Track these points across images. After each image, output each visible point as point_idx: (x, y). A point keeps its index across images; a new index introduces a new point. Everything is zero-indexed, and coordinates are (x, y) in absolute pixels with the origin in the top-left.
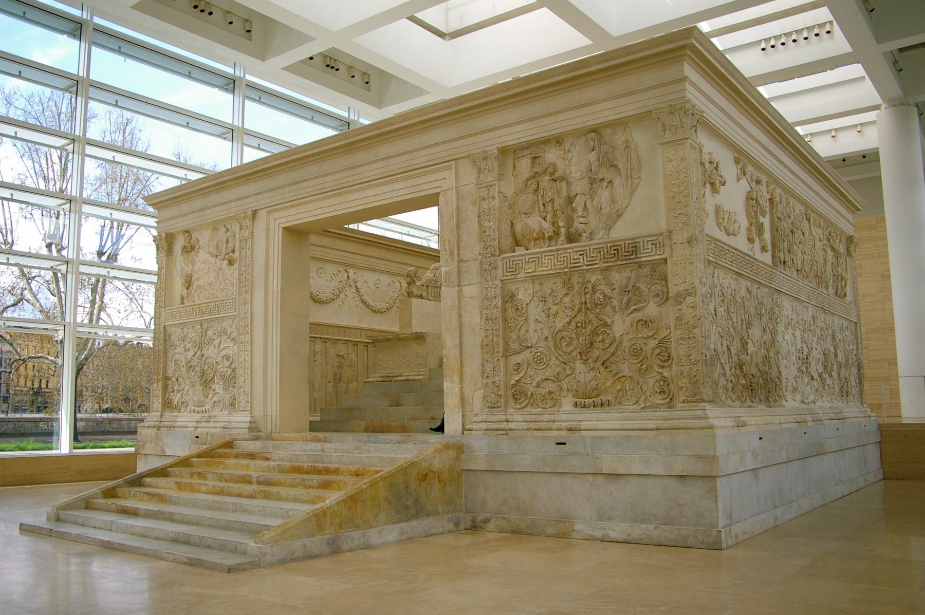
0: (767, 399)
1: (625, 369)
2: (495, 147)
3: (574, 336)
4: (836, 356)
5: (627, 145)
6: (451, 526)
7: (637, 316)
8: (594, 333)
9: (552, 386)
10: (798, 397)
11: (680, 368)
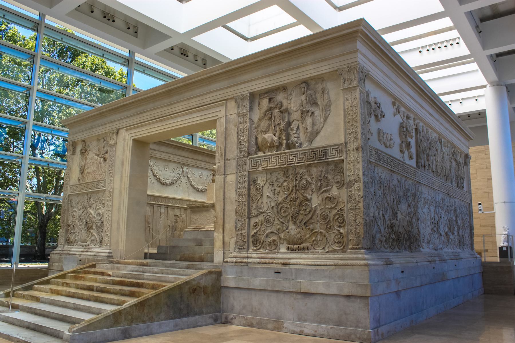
0: (410, 247)
4: (457, 222)
5: (323, 90)
6: (211, 321)
7: (326, 195)
8: (300, 205)
9: (275, 237)
10: (431, 246)
11: (349, 227)
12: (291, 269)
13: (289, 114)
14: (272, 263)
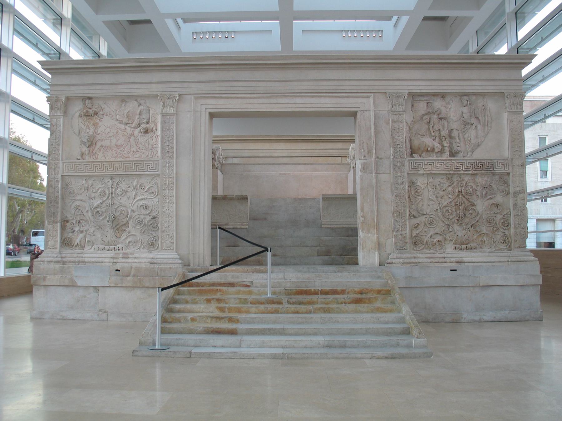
1: (484, 229)
2: (407, 91)
5: (485, 108)
8: (466, 209)
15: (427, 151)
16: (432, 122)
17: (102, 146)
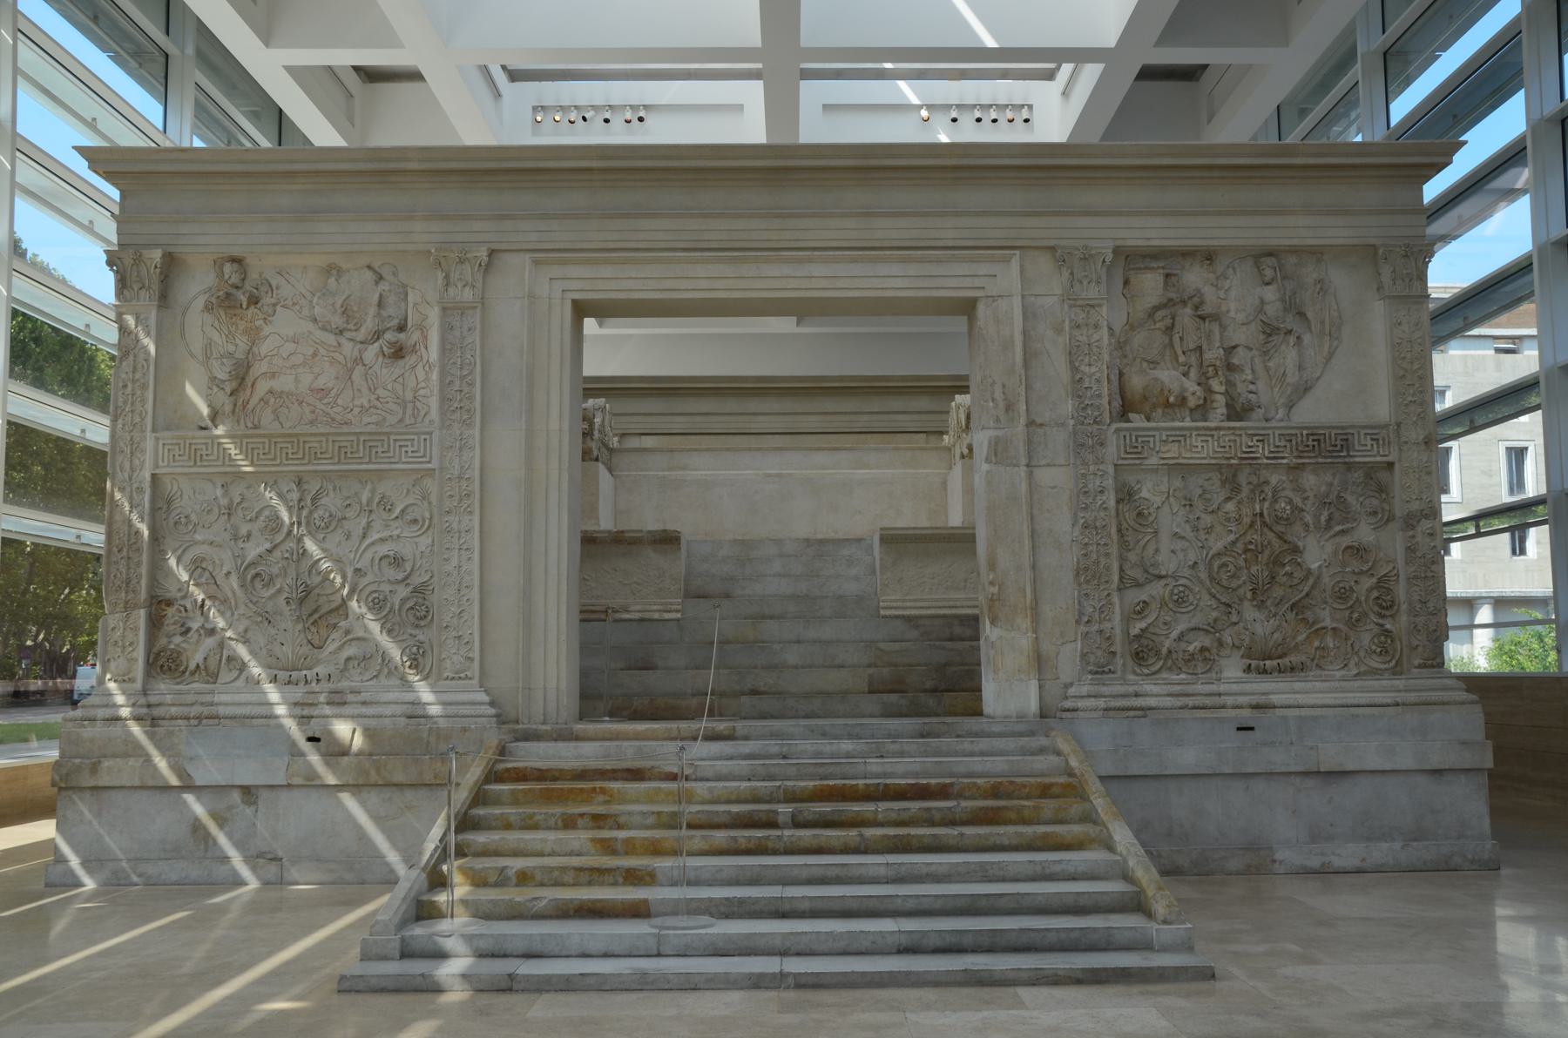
2: (1111, 244)
3: (1242, 564)
5: (1322, 286)
9: (1207, 641)
12: (1284, 718)
13: (1223, 328)
14: (1223, 707)
15: (1168, 405)
16: (1178, 327)
17: (271, 392)
